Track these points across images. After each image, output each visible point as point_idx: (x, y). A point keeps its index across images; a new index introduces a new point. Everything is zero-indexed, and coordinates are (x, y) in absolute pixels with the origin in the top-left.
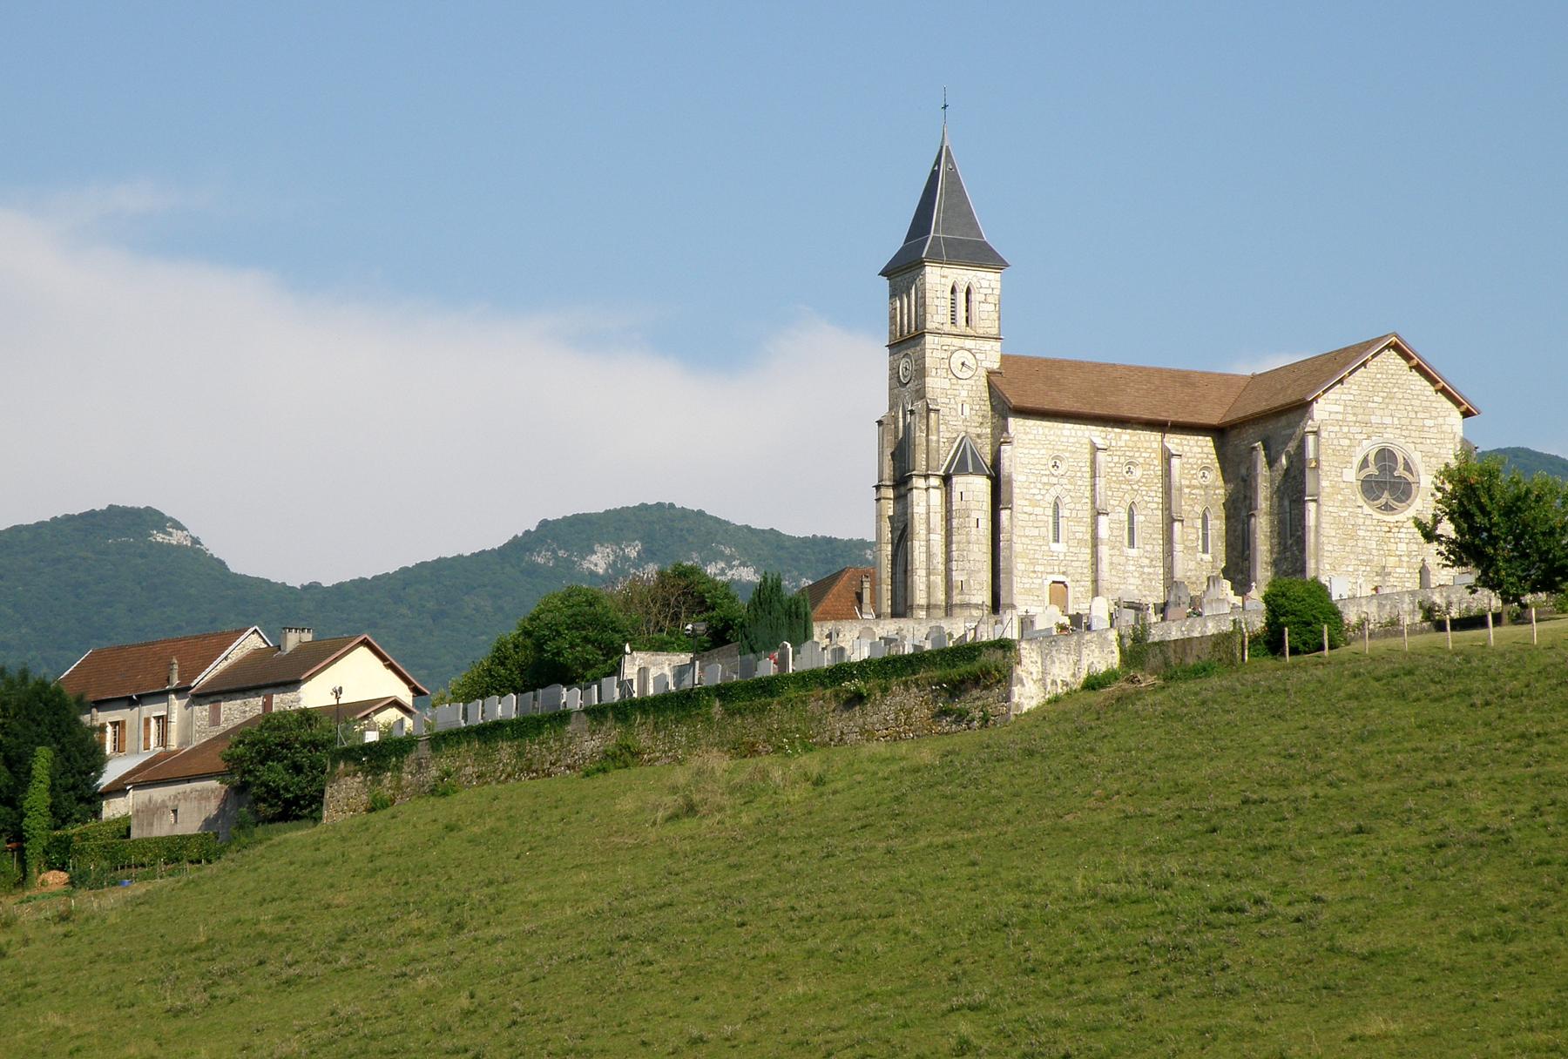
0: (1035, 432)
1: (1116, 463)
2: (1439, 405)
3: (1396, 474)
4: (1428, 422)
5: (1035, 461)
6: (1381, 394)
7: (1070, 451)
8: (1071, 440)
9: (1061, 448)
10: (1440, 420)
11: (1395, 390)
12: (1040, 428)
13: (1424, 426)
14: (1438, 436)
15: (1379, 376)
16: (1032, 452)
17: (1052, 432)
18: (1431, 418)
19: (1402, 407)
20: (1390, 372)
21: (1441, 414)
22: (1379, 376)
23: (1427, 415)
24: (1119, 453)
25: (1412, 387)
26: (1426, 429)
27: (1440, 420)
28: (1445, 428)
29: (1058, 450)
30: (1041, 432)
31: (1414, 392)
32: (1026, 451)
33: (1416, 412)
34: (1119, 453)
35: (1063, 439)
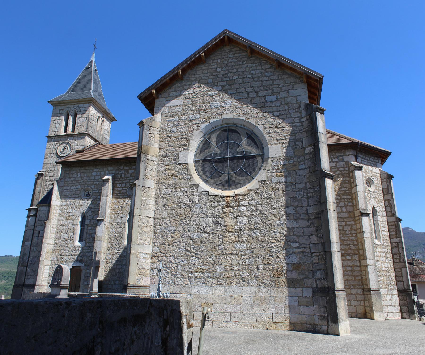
0: (76, 176)
1: (123, 188)
2: (282, 82)
3: (239, 150)
4: (269, 99)
5: (73, 193)
6: (221, 83)
7: (95, 184)
8: (97, 178)
9: (90, 183)
10: (284, 94)
11: (235, 78)
12: (79, 174)
13: (266, 101)
14: (282, 108)
15: (218, 70)
16: (72, 188)
17: (85, 175)
18: (273, 94)
19: (243, 90)
20: (230, 65)
21: (284, 89)
22: (218, 70)
23: (270, 92)
24: (125, 181)
25: (253, 72)
26: (267, 104)
27: (284, 94)
28: (289, 100)
29: (88, 185)
30: (79, 175)
31: (254, 76)
32: (69, 188)
33: (257, 92)
34: (125, 181)
35: (92, 178)
